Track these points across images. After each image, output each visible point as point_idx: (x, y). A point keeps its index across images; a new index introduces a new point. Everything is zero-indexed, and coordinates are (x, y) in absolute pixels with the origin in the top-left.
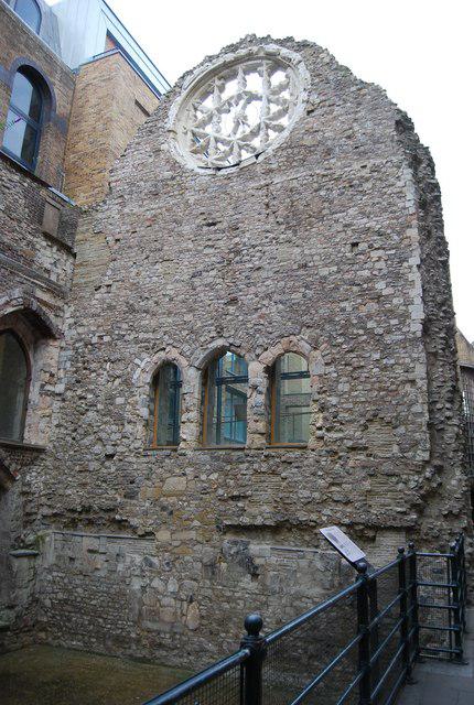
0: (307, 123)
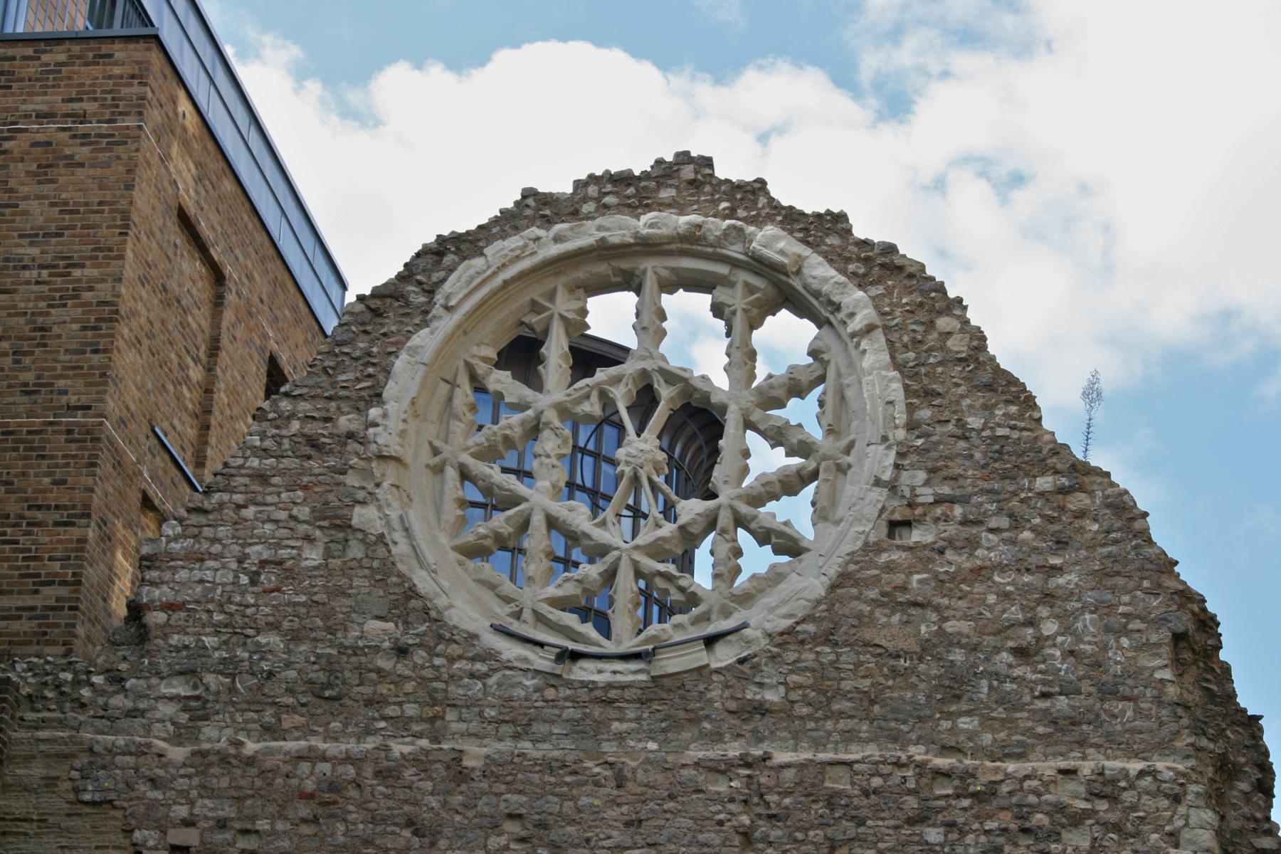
0: (889, 567)
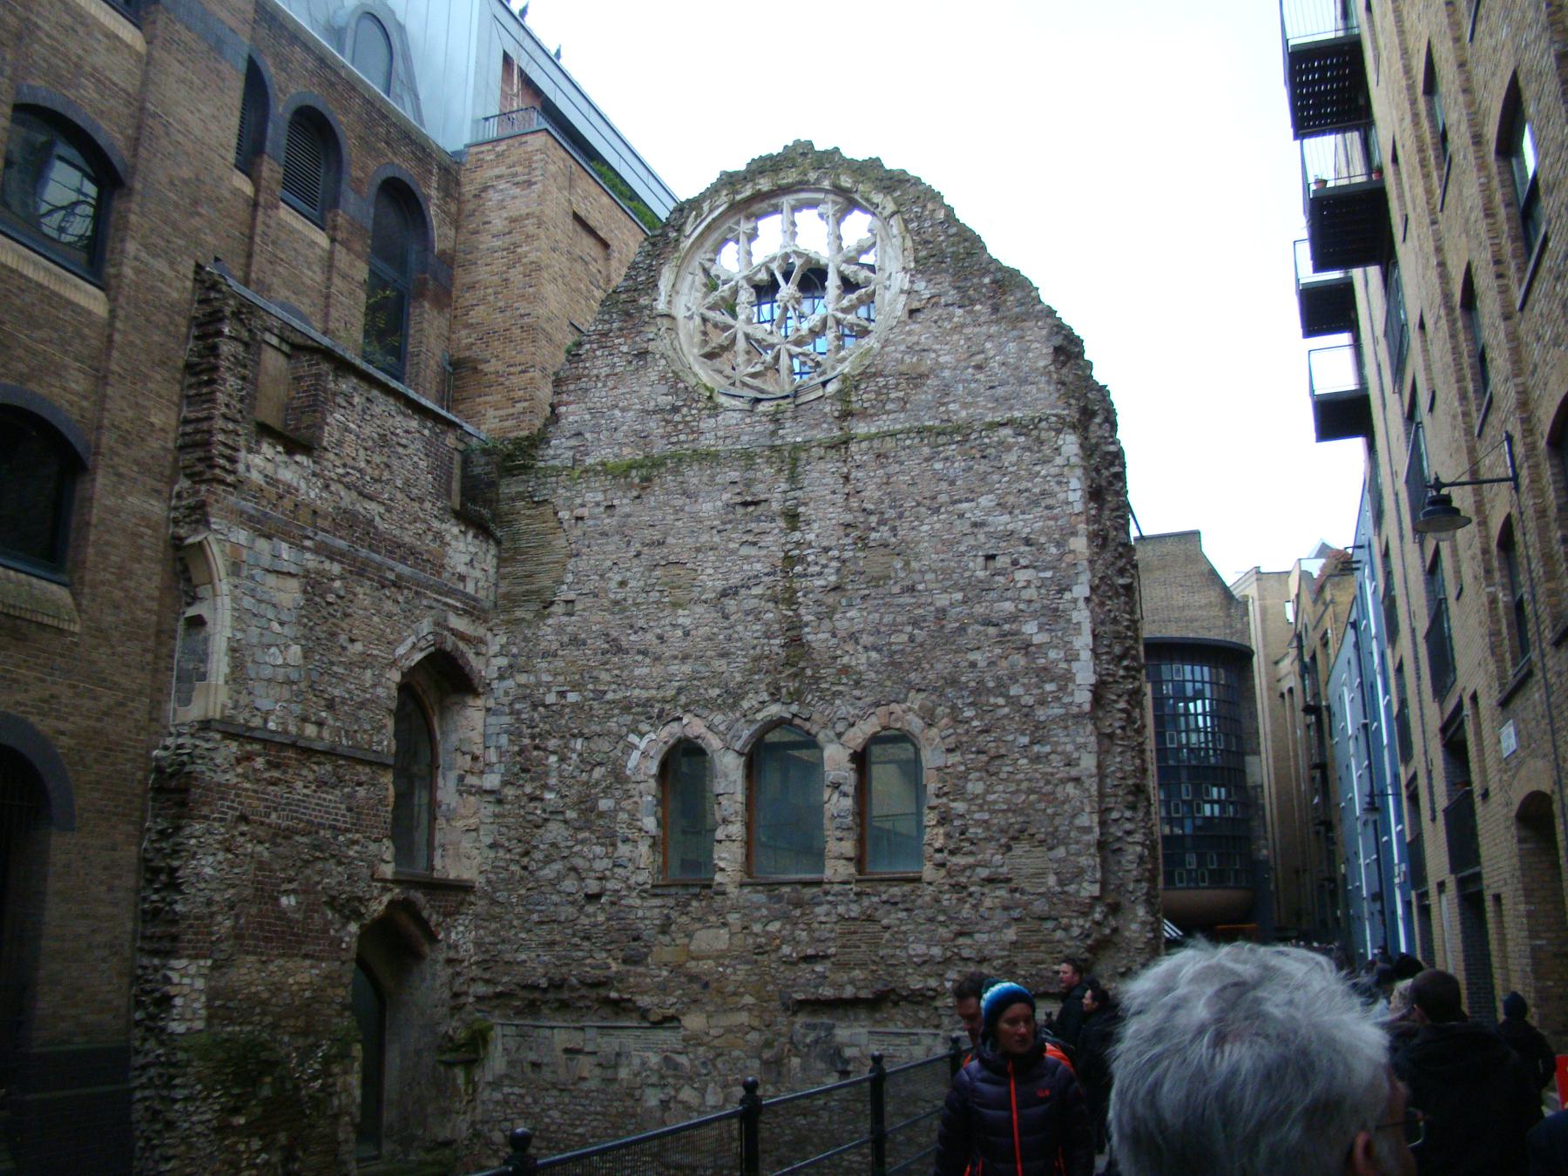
0: (910, 333)
